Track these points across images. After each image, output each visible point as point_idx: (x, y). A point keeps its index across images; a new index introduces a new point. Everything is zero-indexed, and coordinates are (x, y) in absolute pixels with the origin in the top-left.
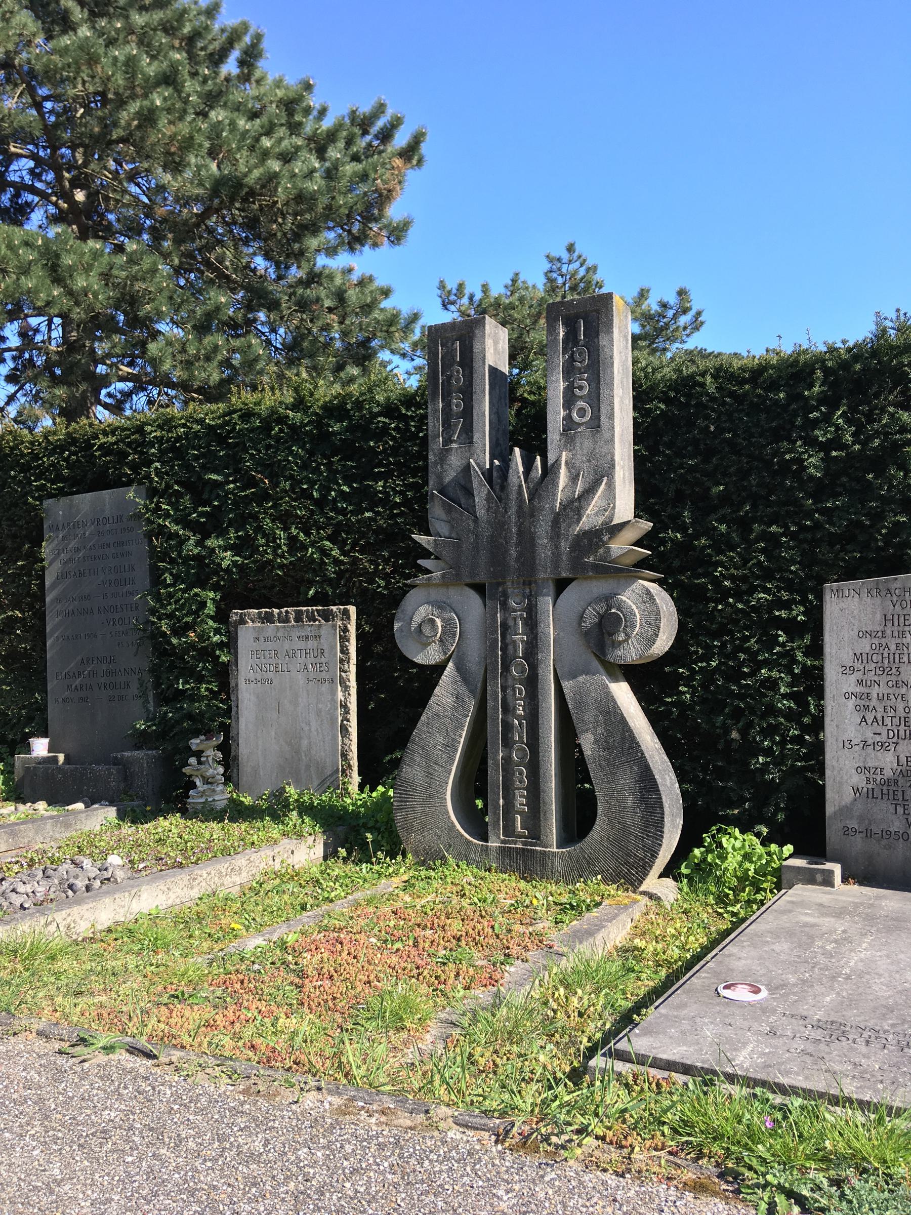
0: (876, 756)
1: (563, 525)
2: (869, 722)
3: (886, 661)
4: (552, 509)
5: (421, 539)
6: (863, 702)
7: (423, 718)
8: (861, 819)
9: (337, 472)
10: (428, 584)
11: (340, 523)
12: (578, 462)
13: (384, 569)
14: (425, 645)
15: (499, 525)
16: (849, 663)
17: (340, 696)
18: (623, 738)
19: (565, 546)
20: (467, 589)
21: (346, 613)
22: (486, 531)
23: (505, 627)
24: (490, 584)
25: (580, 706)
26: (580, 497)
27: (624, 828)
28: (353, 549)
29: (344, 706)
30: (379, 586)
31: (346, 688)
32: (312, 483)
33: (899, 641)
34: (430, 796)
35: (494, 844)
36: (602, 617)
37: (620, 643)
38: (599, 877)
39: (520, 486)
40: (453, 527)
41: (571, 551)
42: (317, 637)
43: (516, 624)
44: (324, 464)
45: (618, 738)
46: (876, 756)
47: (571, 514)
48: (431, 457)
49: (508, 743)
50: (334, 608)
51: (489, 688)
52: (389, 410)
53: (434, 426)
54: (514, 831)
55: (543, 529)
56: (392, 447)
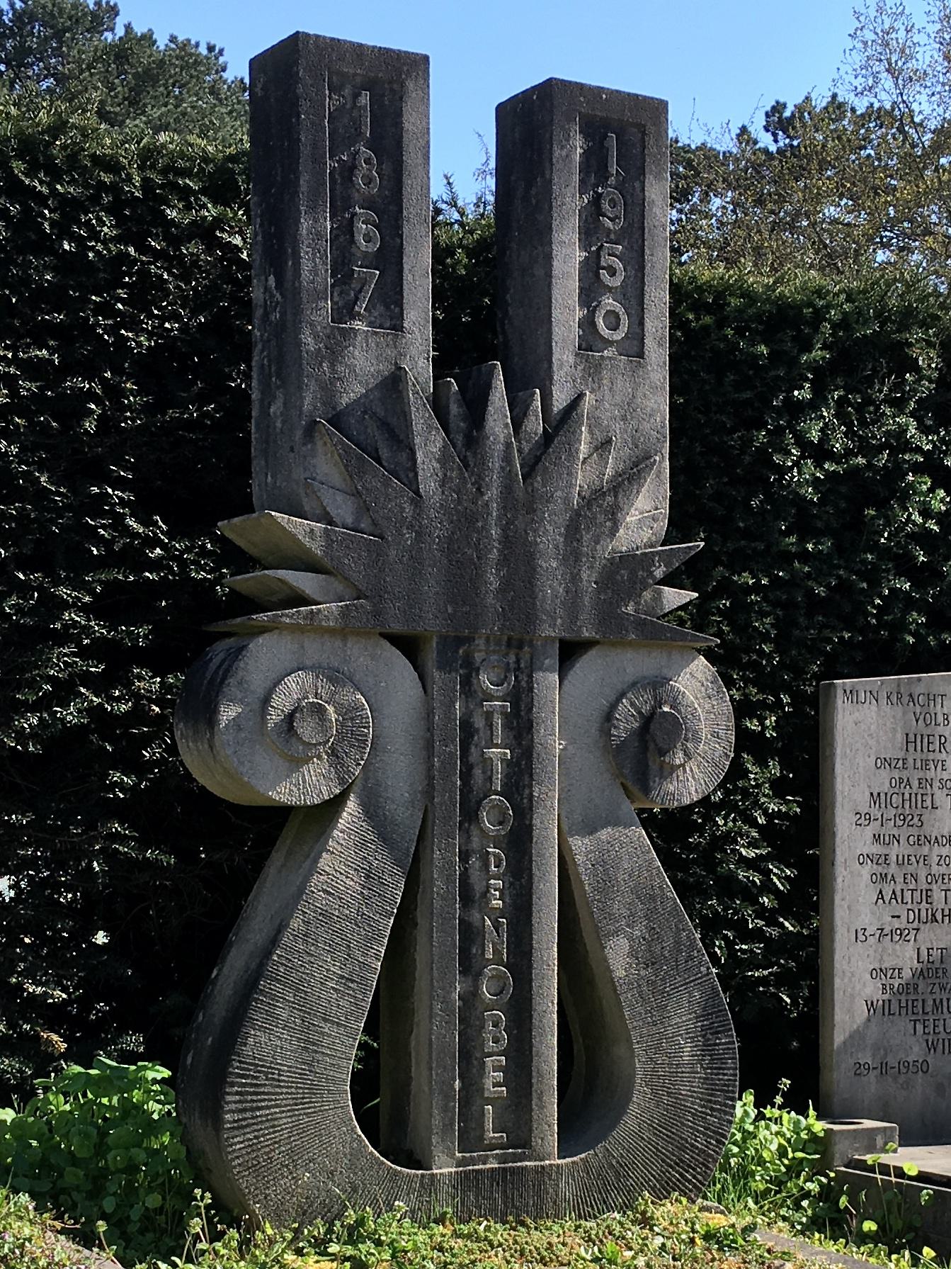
0: (894, 950)
1: (587, 537)
2: (887, 898)
3: (907, 805)
4: (567, 500)
6: (880, 869)
8: (876, 1048)
10: (312, 627)
14: (297, 762)
15: (466, 519)
16: (864, 810)
18: (678, 942)
19: (589, 577)
20: (387, 644)
22: (439, 530)
23: (468, 730)
25: (606, 885)
27: (677, 1104)
33: (921, 774)
35: (444, 1169)
36: (648, 721)
37: (674, 768)
41: (598, 591)
43: (490, 726)
45: (669, 943)
46: (894, 950)
47: (601, 518)
49: (470, 966)
54: (481, 1138)
55: (549, 537)
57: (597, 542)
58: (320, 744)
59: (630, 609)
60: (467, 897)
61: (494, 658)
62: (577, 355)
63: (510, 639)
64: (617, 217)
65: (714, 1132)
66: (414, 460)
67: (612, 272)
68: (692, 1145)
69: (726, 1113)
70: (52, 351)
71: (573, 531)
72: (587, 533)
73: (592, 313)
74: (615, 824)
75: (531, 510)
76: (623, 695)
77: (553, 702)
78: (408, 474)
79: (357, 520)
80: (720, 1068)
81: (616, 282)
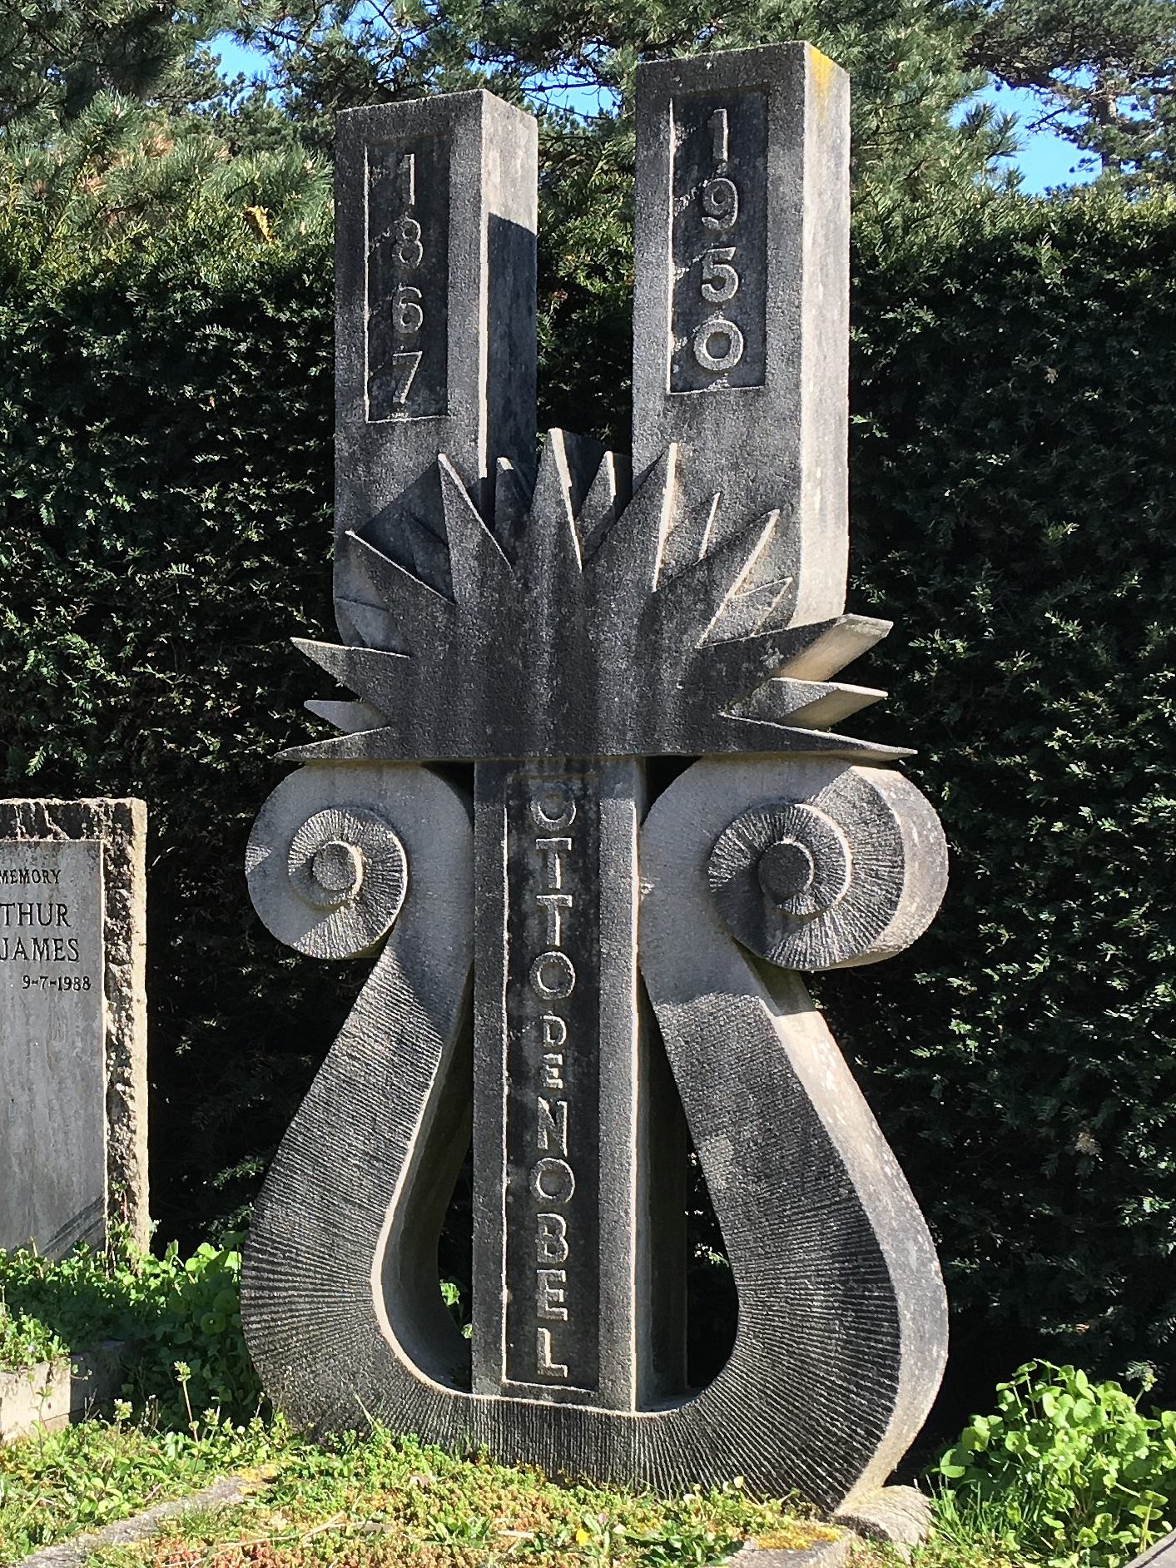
1: (669, 627)
4: (642, 584)
5: (314, 649)
7: (317, 1088)
9: (99, 459)
10: (333, 762)
11: (107, 588)
12: (707, 468)
13: (218, 707)
14: (323, 911)
15: (510, 622)
17: (107, 1021)
18: (807, 1152)
19: (672, 679)
21: (123, 817)
22: (476, 637)
23: (519, 870)
24: (486, 767)
25: (702, 1071)
26: (711, 557)
27: (803, 1366)
28: (139, 657)
29: (117, 1047)
30: (205, 751)
31: (121, 1004)
32: (38, 488)
34: (332, 1278)
36: (758, 855)
37: (803, 920)
38: (739, 1481)
39: (563, 526)
40: (393, 623)
41: (684, 695)
42: (50, 875)
44: (67, 440)
47: (688, 600)
48: (342, 445)
49: (522, 1157)
50: (92, 803)
51: (478, 1020)
52: (234, 306)
53: (350, 369)
55: (617, 636)
56: (236, 402)
57: (685, 631)
58: (342, 891)
59: (736, 711)
60: (521, 1072)
61: (549, 785)
62: (667, 398)
63: (569, 761)
64: (726, 213)
65: (861, 1418)
66: (449, 560)
67: (718, 282)
68: (828, 1431)
69: (881, 1396)
70: (312, 479)
71: (650, 619)
72: (670, 620)
73: (691, 341)
74: (722, 989)
75: (591, 599)
76: (729, 825)
77: (628, 835)
78: (441, 580)
79: (388, 638)
80: (869, 1331)
81: (730, 293)
